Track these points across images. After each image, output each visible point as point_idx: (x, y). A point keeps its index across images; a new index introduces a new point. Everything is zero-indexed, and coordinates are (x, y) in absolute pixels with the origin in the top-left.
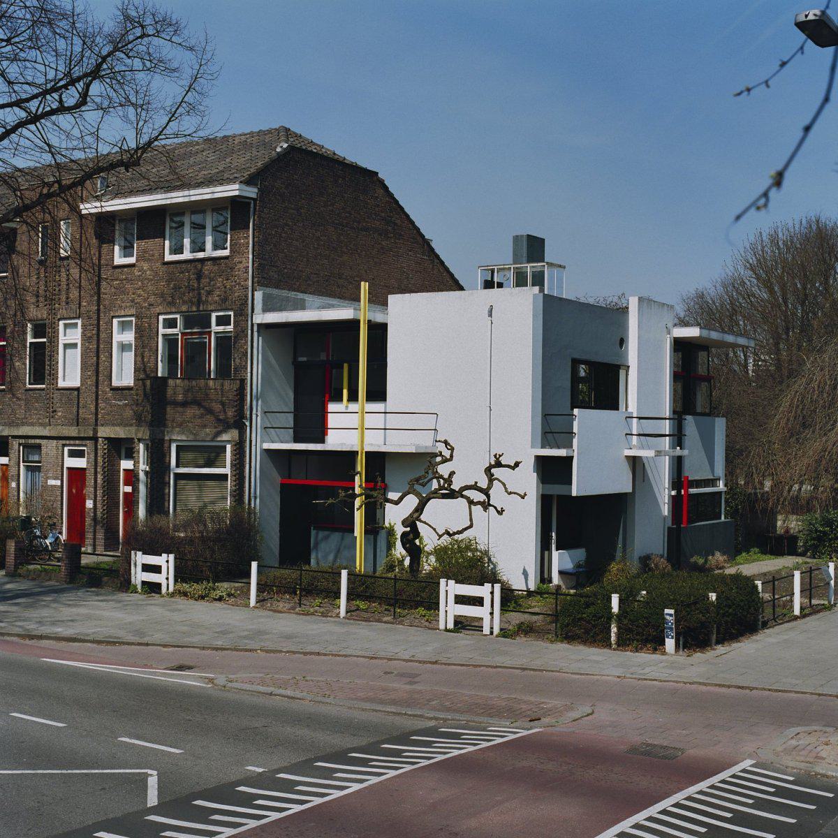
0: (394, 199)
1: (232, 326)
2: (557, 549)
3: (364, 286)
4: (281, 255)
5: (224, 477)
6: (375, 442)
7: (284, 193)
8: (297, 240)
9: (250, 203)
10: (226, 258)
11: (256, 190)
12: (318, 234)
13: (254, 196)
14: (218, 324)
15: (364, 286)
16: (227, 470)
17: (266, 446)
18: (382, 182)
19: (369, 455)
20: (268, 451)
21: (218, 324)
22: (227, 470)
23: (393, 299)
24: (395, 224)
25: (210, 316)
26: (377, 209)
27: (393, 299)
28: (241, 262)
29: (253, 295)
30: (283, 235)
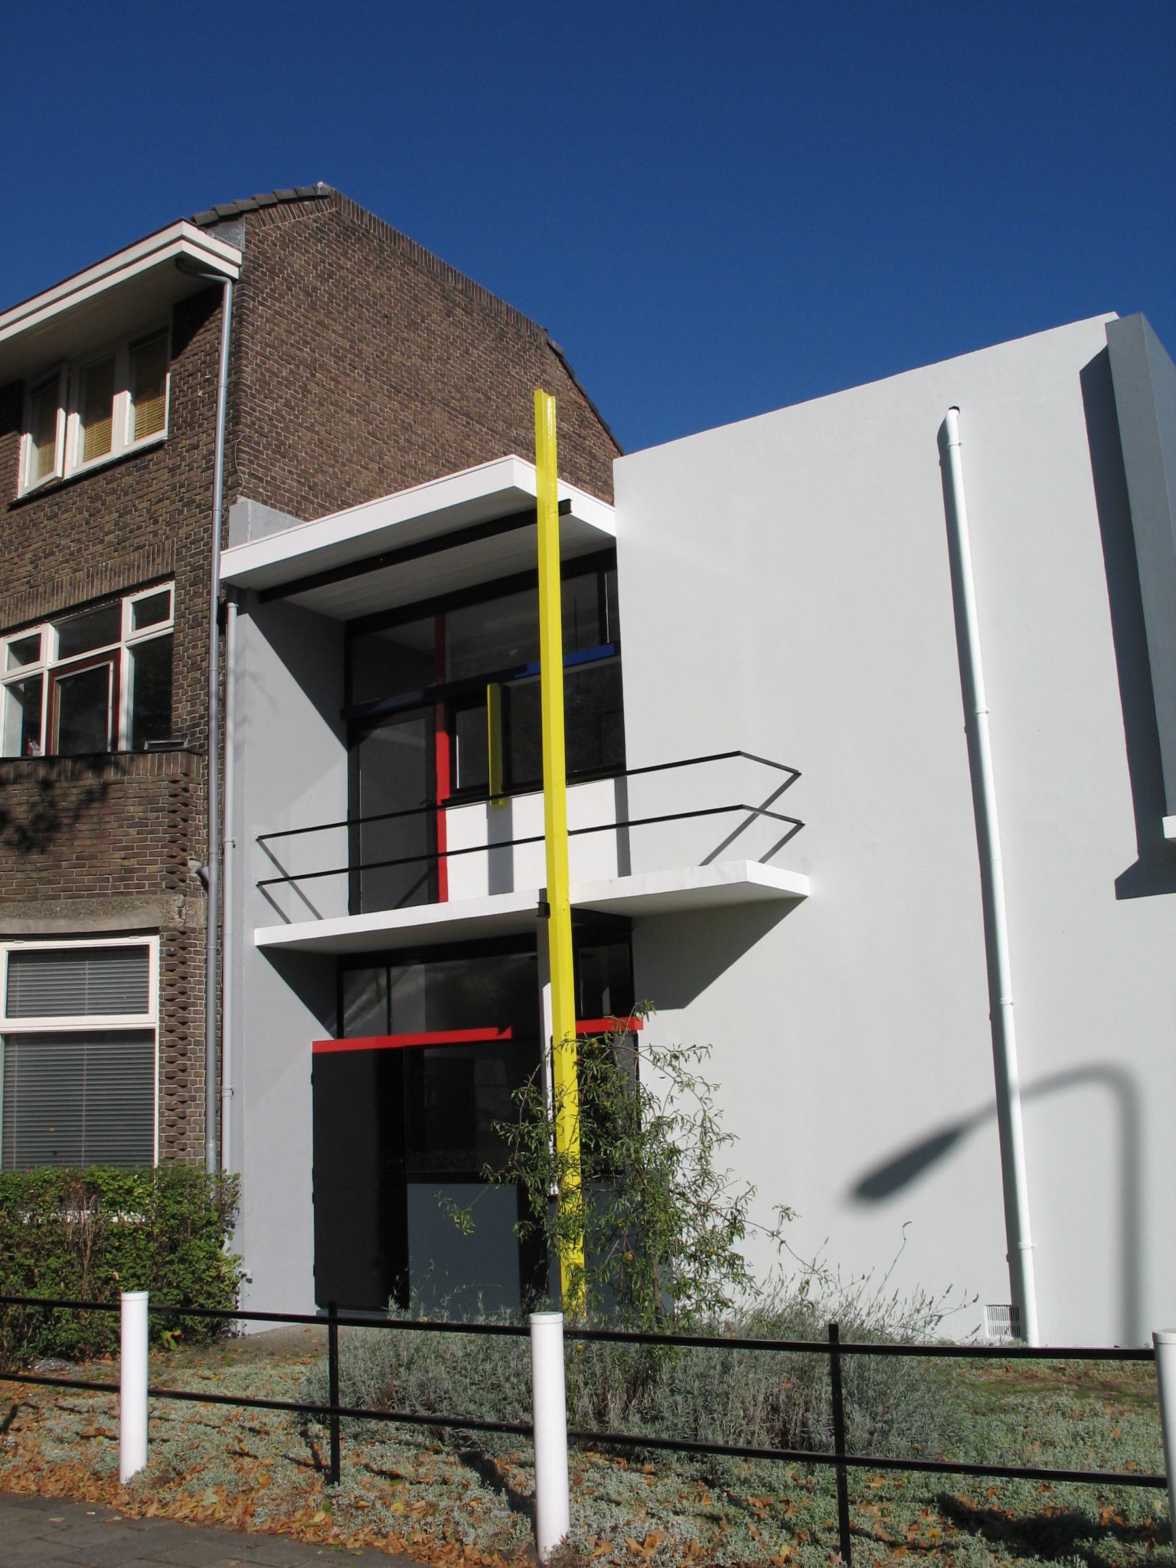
1: (170, 622)
3: (547, 408)
5: (146, 1035)
6: (593, 877)
7: (315, 289)
8: (350, 412)
9: (221, 287)
10: (159, 446)
11: (237, 256)
13: (234, 272)
14: (140, 623)
15: (547, 408)
16: (151, 1019)
19: (588, 922)
21: (140, 623)
22: (151, 1019)
23: (627, 469)
25: (119, 606)
27: (623, 467)
28: (196, 447)
29: (225, 522)
30: (312, 386)
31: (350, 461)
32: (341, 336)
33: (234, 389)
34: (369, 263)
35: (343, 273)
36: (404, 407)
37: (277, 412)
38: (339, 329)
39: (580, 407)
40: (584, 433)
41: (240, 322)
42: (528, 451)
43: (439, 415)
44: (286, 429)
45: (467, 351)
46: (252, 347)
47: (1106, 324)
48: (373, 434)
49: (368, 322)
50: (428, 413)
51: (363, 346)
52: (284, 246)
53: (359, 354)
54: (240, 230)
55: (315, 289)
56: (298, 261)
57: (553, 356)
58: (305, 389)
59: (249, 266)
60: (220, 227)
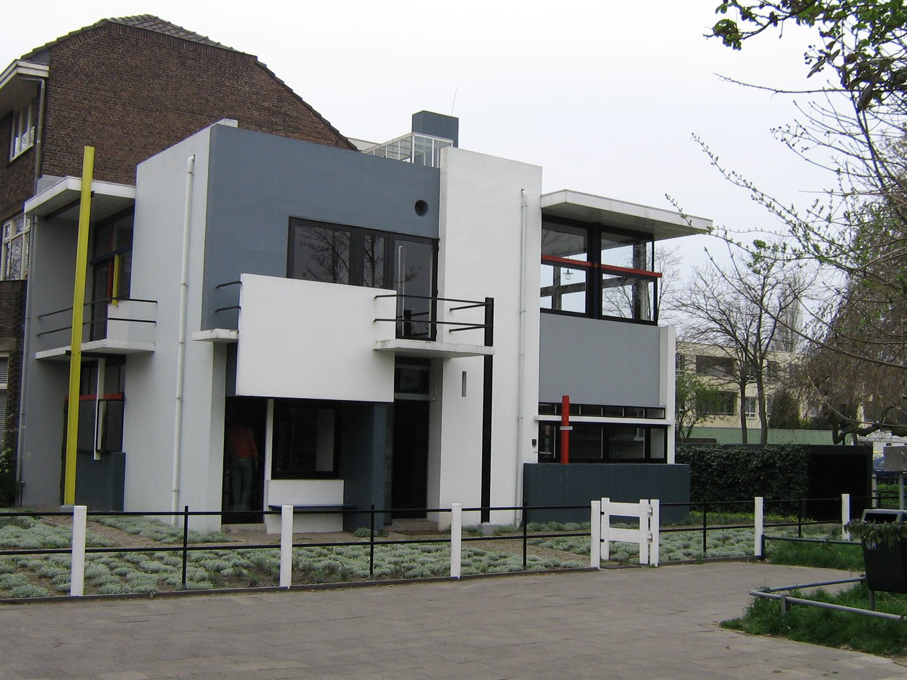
0: (285, 86)
2: (274, 476)
3: (89, 153)
7: (93, 73)
8: (113, 125)
11: (47, 68)
12: (150, 121)
13: (46, 75)
15: (89, 153)
17: (41, 355)
18: (263, 67)
20: (42, 361)
23: (143, 169)
24: (289, 116)
26: (254, 97)
30: (89, 119)
36: (147, 116)
37: (68, 134)
38: (107, 88)
39: (279, 91)
42: (78, 173)
44: (72, 141)
45: (194, 81)
48: (127, 133)
50: (165, 116)
52: (74, 57)
53: (120, 98)
55: (93, 73)
56: (82, 62)
57: (260, 70)
58: (85, 120)
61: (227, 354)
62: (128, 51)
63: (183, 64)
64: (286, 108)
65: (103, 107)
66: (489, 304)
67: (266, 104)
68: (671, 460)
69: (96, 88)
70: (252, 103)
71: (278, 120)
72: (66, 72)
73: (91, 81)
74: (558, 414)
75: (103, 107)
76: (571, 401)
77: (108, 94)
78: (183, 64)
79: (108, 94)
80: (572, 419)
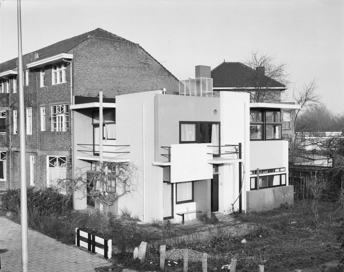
4: (86, 81)
11: (72, 55)
18: (141, 48)
26: (138, 59)
30: (87, 73)
31: (95, 82)
32: (93, 62)
33: (73, 77)
34: (98, 47)
35: (93, 51)
39: (146, 56)
40: (147, 61)
41: (73, 65)
43: (113, 69)
46: (75, 70)
47: (196, 66)
49: (98, 57)
51: (97, 62)
54: (72, 51)
59: (75, 56)
60: (68, 52)
61: (167, 169)
62: (98, 47)
63: (115, 49)
64: (149, 62)
65: (91, 68)
66: (240, 145)
67: (142, 61)
68: (287, 184)
69: (88, 61)
70: (138, 61)
71: (146, 66)
72: (79, 56)
73: (87, 59)
74: (256, 174)
75: (91, 68)
76: (260, 169)
77: (92, 63)
78: (115, 49)
79: (92, 63)
80: (261, 175)
